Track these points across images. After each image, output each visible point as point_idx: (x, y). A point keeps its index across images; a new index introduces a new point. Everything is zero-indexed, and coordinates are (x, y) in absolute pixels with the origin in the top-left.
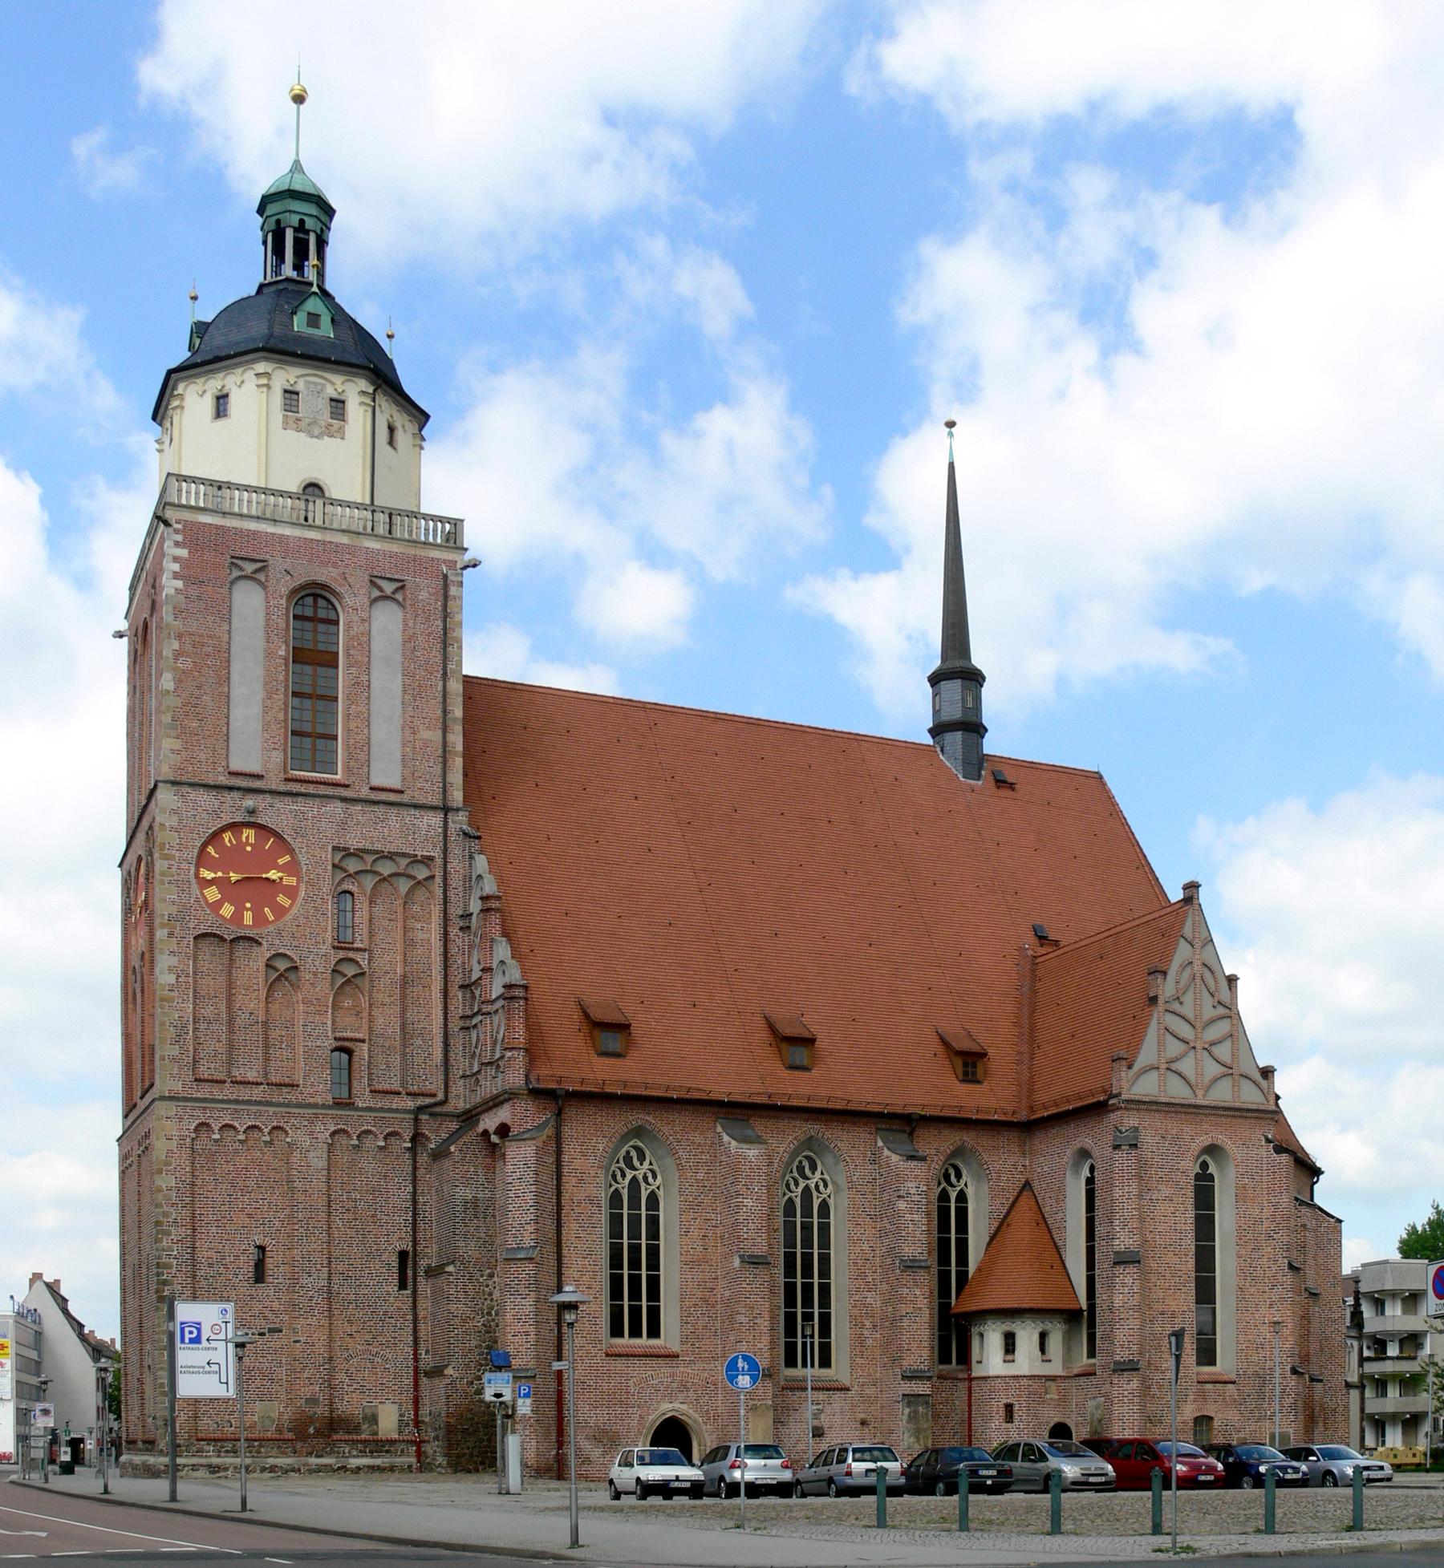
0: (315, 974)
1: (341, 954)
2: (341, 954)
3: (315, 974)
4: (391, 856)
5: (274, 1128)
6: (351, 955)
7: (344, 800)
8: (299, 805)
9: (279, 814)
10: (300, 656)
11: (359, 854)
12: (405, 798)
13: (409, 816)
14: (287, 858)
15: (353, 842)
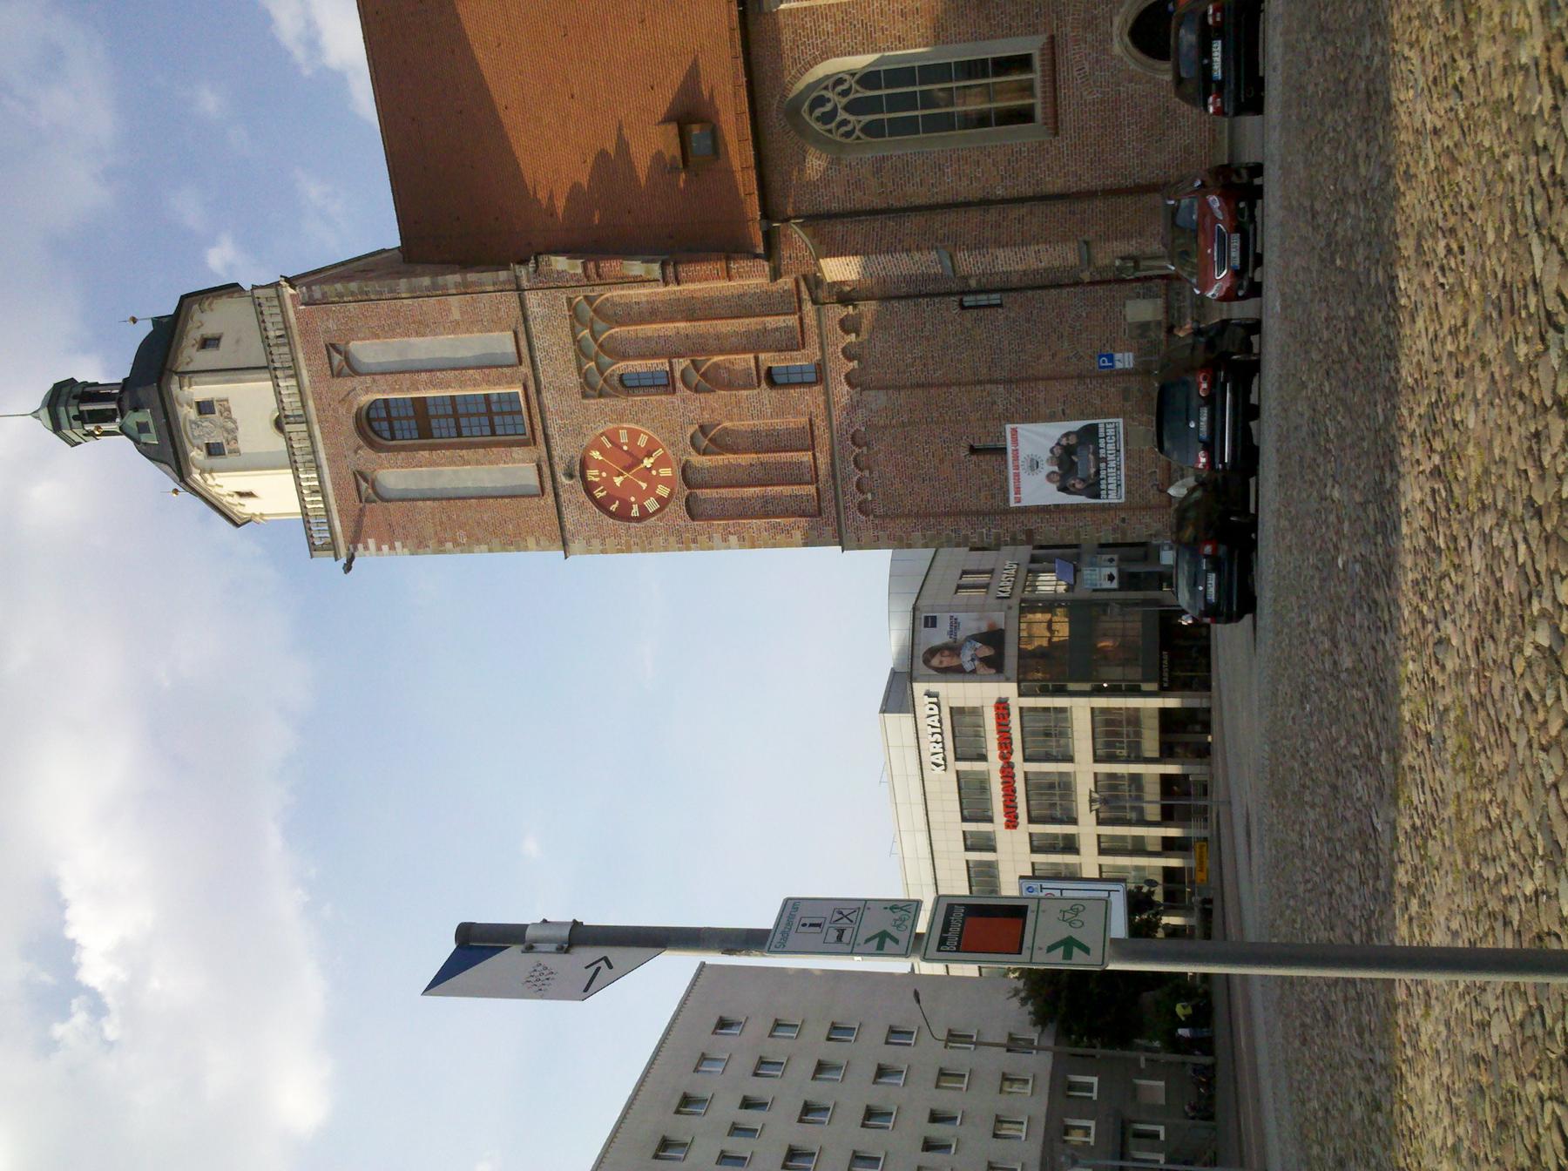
0: (703, 409)
1: (679, 385)
2: (679, 385)
3: (703, 409)
4: (577, 341)
5: (854, 443)
6: (677, 375)
7: (538, 392)
8: (552, 431)
9: (565, 449)
10: (425, 432)
11: (584, 375)
12: (521, 329)
13: (535, 329)
14: (604, 439)
15: (574, 380)
